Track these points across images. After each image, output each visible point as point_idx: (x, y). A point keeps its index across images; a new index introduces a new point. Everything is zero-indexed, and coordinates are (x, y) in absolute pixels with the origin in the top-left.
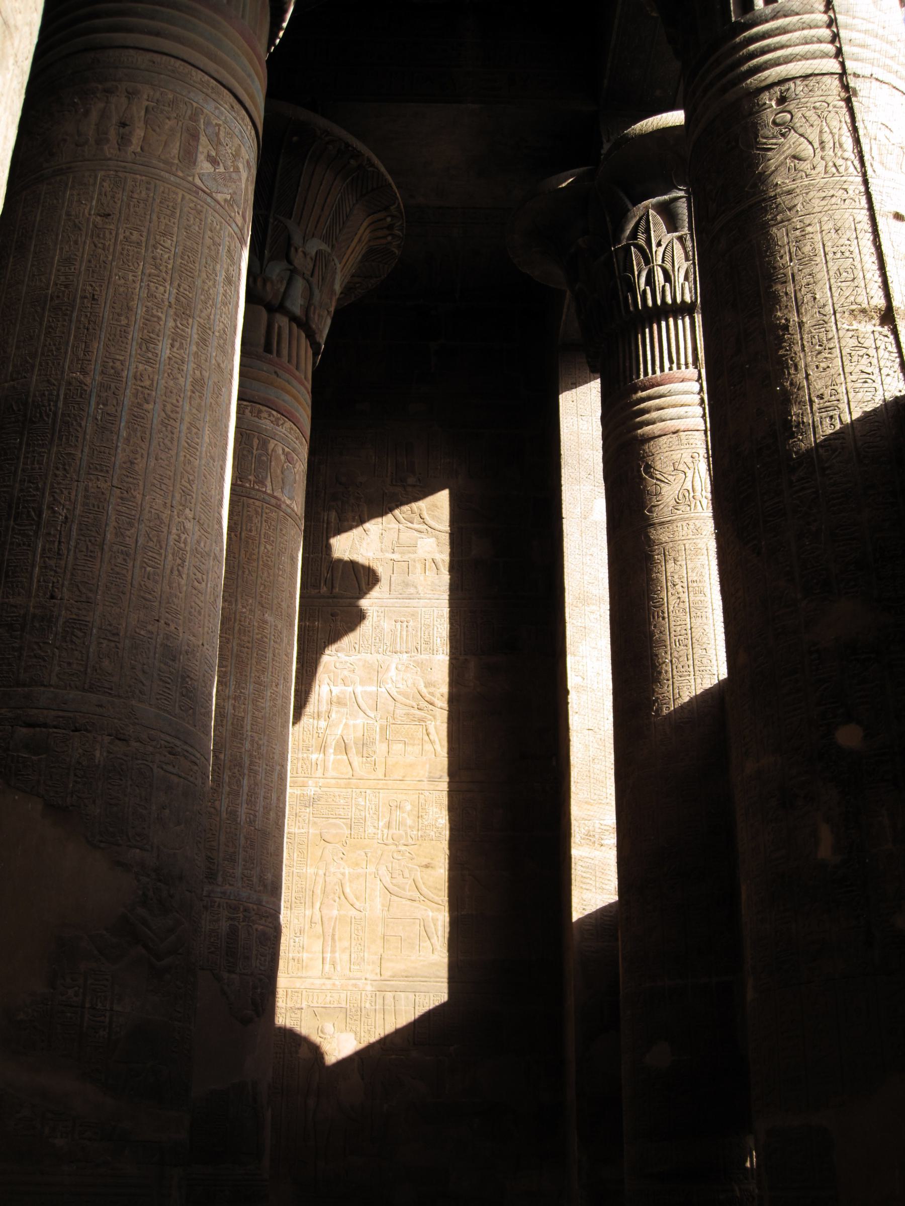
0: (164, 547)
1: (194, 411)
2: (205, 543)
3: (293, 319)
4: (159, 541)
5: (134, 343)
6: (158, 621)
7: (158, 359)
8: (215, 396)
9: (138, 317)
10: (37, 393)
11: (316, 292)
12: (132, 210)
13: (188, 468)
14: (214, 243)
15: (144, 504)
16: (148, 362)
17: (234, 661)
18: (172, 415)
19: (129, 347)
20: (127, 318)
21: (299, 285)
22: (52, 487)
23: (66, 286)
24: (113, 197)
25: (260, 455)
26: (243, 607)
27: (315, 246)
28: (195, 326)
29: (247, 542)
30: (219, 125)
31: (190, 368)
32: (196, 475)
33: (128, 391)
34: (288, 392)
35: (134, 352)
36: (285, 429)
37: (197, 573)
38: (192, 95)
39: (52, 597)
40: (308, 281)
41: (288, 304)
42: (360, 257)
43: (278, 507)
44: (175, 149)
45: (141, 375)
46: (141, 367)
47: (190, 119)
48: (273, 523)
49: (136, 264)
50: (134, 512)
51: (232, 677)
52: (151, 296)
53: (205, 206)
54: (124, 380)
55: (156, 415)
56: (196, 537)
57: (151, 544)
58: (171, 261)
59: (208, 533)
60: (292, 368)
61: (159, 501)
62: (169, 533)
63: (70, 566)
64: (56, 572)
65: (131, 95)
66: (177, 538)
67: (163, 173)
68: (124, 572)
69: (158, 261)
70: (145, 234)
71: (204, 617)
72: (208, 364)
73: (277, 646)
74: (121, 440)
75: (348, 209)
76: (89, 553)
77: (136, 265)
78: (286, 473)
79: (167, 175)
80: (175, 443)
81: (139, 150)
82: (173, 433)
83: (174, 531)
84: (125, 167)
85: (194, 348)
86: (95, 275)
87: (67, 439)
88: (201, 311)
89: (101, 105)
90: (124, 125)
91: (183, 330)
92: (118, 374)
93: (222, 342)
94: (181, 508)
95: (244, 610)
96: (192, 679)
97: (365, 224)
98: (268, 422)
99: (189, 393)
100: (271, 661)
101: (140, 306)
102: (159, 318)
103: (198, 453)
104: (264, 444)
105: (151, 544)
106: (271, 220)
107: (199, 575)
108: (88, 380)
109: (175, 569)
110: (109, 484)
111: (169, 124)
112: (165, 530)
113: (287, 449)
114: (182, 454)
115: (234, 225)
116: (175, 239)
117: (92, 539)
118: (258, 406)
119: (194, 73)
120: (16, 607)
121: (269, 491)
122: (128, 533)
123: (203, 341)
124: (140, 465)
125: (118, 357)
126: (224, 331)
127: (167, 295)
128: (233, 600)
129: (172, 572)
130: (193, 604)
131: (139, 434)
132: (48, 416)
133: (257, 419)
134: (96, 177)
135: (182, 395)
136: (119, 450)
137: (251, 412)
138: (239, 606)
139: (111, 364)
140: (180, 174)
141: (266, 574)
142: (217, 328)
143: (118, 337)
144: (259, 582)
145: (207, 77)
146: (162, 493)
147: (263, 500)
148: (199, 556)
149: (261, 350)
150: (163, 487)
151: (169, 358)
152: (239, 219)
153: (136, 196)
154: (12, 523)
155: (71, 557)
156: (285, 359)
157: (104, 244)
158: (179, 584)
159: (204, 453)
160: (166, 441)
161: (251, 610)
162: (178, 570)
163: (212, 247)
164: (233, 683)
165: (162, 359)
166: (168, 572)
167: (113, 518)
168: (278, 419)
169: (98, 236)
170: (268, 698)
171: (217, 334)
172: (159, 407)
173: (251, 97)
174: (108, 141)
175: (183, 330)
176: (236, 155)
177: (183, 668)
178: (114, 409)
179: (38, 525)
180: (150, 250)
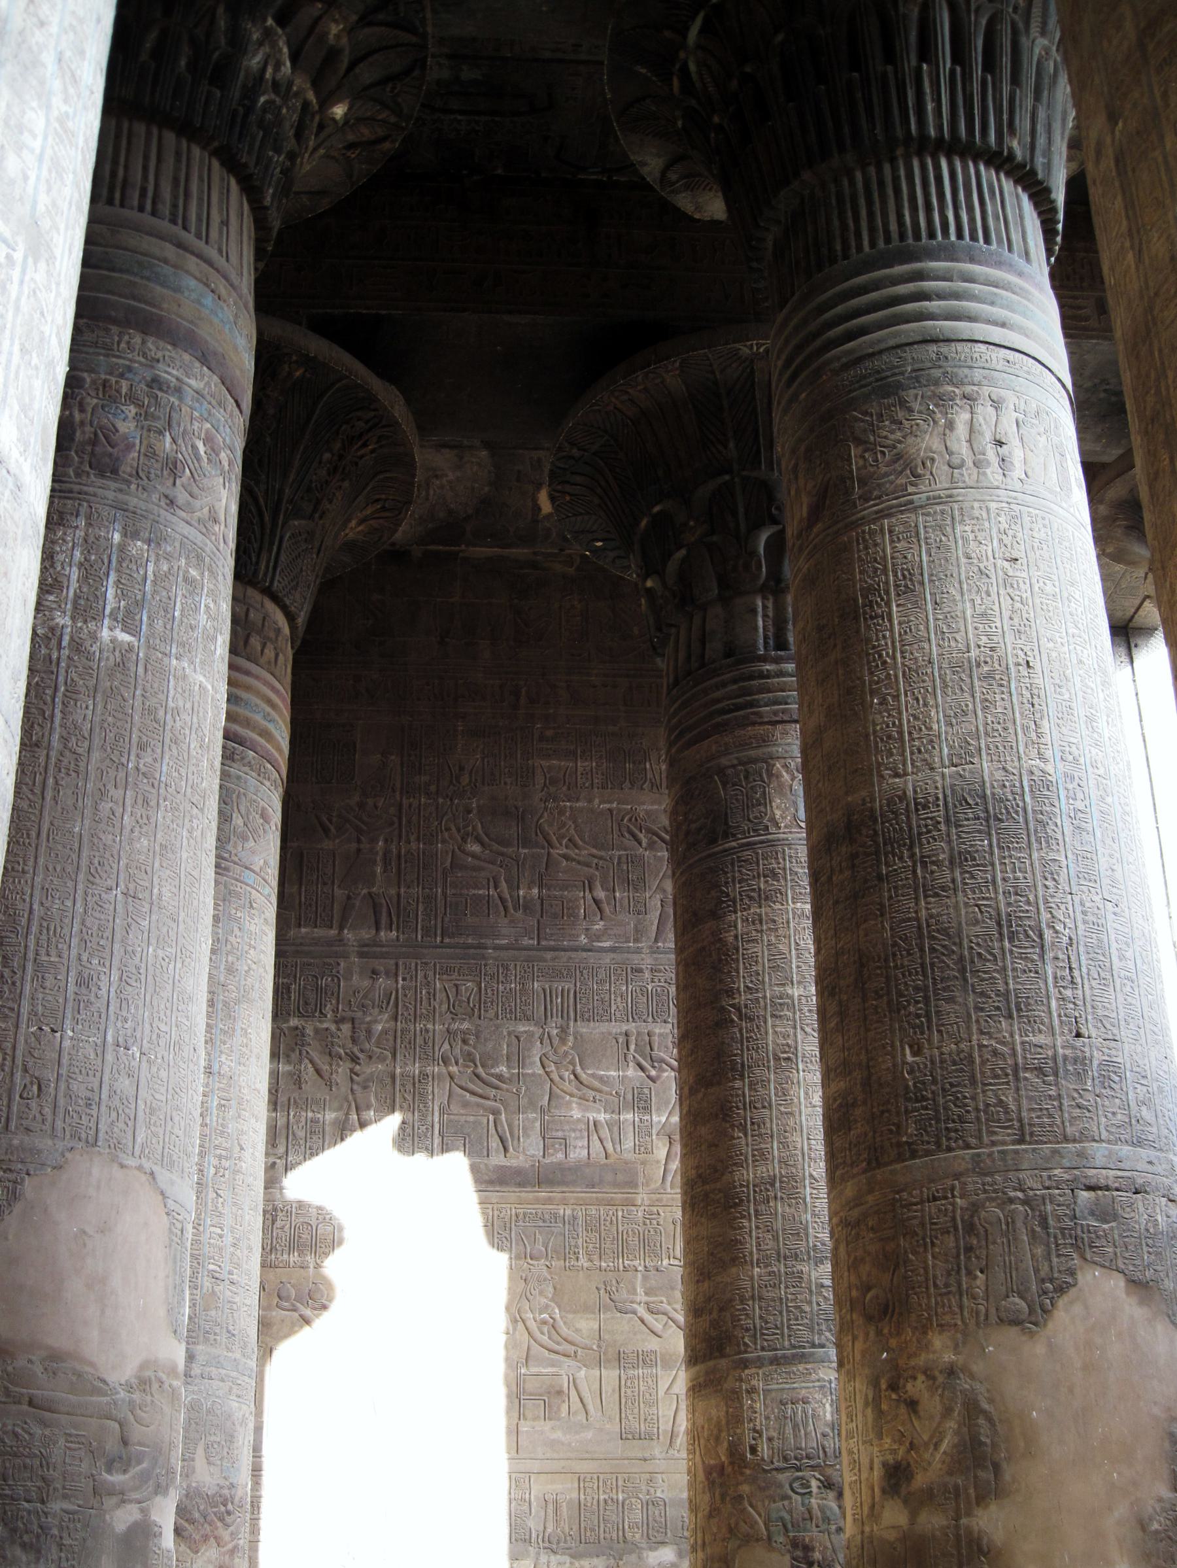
10: (995, 784)
23: (992, 649)
39: (1078, 1035)
64: (1074, 1003)
67: (1052, 505)
79: (1055, 508)
86: (1023, 636)
87: (1047, 842)
90: (1000, 443)
108: (1049, 768)
120: (1041, 1047)
132: (1017, 812)
154: (1007, 944)
155: (1086, 986)
174: (989, 463)
179: (1042, 947)
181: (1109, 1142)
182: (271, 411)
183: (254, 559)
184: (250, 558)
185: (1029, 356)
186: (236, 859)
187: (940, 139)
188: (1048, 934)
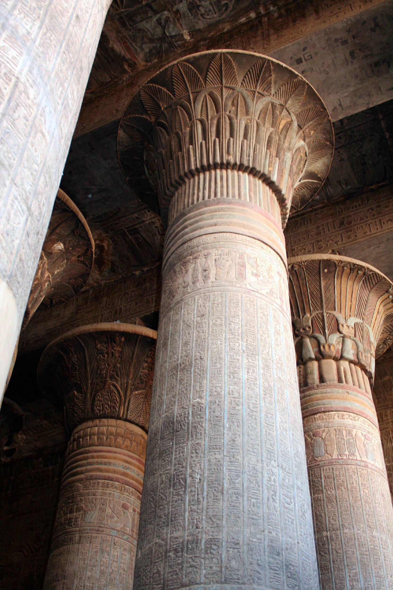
0: (261, 485)
1: (268, 405)
2: (289, 480)
3: (351, 362)
4: (257, 483)
5: (226, 376)
6: (263, 531)
7: (241, 381)
8: (280, 395)
9: (226, 362)
10: (178, 415)
11: (360, 345)
12: (215, 309)
13: (269, 437)
14: (264, 315)
15: (244, 462)
16: (235, 384)
17: (360, 565)
18: (254, 410)
19: (223, 378)
20: (220, 364)
21: (349, 343)
22: (191, 464)
24: (204, 306)
25: (349, 440)
26: (358, 530)
27: (352, 321)
28: (260, 360)
29: (352, 491)
30: (256, 258)
31: (261, 382)
32: (275, 441)
33: (226, 402)
34: (356, 401)
35: (226, 380)
36: (360, 422)
37: (286, 498)
38: (238, 247)
39: (197, 528)
40: (353, 340)
41: (345, 355)
42: (382, 321)
43: (367, 466)
44: (233, 274)
45: (232, 392)
46: (231, 387)
47: (239, 258)
48: (365, 477)
49: (221, 336)
50: (239, 469)
51: (361, 575)
52: (232, 349)
53: (255, 298)
54: (223, 396)
55: (244, 411)
56: (281, 477)
57: (252, 485)
58: (240, 329)
59: (290, 473)
60: (357, 388)
61: (254, 459)
62: (263, 477)
63: (205, 508)
64: (198, 512)
65: (206, 256)
66: (269, 479)
67: (228, 287)
68: (238, 504)
69: (233, 331)
70: (223, 319)
71: (296, 525)
72: (272, 378)
73: (385, 551)
74: (226, 429)
75: (366, 298)
76: (215, 498)
77: (221, 336)
78: (367, 446)
79: (231, 288)
80: (259, 424)
81: (214, 280)
82: (256, 419)
83: (266, 475)
84: (208, 290)
85: (262, 371)
87: (196, 436)
88: (263, 351)
89: (193, 266)
90: (205, 270)
91: (253, 363)
92: (219, 394)
93: (279, 365)
94: (268, 461)
95: (359, 532)
96: (293, 566)
97: (378, 303)
98: (350, 420)
99: (263, 396)
100: (383, 561)
101: (226, 356)
102: (238, 360)
103: (274, 428)
104: (349, 433)
105: (252, 485)
106: (325, 314)
107: (288, 500)
108: (203, 401)
109: (270, 497)
110: (222, 455)
111: (228, 264)
112: (260, 475)
113: (364, 433)
114: (264, 430)
115: (275, 304)
116: (240, 318)
117: (216, 489)
118: (341, 412)
119: (237, 237)
120: (177, 538)
121: (359, 458)
122: (237, 481)
123: (267, 367)
124: (239, 441)
125: (218, 385)
126: (280, 359)
127: (240, 347)
128: (351, 527)
129: (268, 500)
130: (287, 518)
131: (235, 424)
132: (184, 426)
133: (342, 420)
134: (195, 299)
135: (258, 398)
136: (225, 435)
137: (338, 417)
138: (356, 530)
139: (215, 389)
140: (239, 285)
141: (368, 507)
142: (275, 359)
143: (216, 375)
144: (364, 513)
145: (245, 237)
146: (255, 454)
147: (357, 465)
148: (286, 488)
149: (336, 382)
150: (255, 450)
151: (248, 379)
152: (278, 301)
153: (216, 302)
154: (172, 489)
156: (351, 383)
157: (203, 330)
158: (274, 507)
159: (278, 428)
160: (253, 425)
161: (363, 531)
162: (273, 498)
163: (263, 317)
164: (362, 579)
165: (243, 381)
166: (265, 500)
167: (227, 474)
168: (355, 417)
169: (199, 327)
170: (387, 585)
171: (275, 361)
172: (245, 406)
173: (273, 241)
174: (198, 280)
175: (253, 363)
176: (270, 269)
177: (286, 559)
178: (219, 414)
179: (185, 487)
180: (228, 326)
181: (205, 583)
182: (117, 355)
183: (117, 410)
184: (116, 409)
185: (227, 232)
186: (107, 526)
187: (197, 169)
188: (189, 480)
